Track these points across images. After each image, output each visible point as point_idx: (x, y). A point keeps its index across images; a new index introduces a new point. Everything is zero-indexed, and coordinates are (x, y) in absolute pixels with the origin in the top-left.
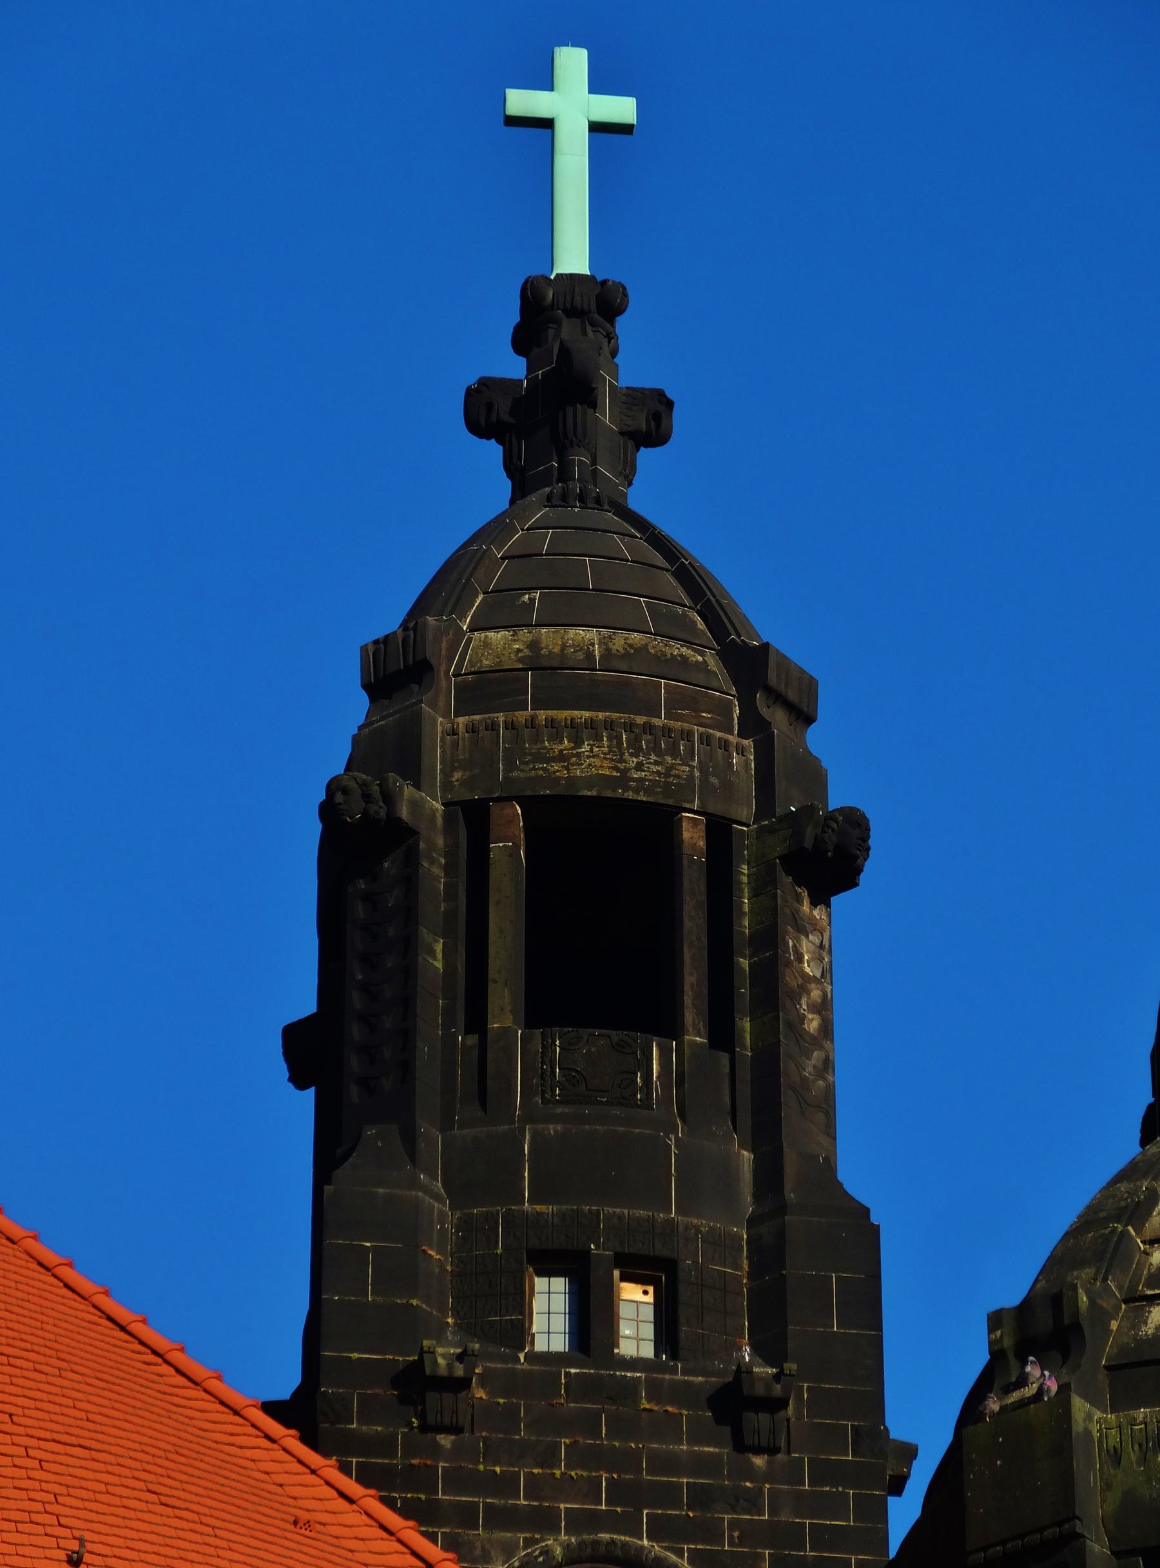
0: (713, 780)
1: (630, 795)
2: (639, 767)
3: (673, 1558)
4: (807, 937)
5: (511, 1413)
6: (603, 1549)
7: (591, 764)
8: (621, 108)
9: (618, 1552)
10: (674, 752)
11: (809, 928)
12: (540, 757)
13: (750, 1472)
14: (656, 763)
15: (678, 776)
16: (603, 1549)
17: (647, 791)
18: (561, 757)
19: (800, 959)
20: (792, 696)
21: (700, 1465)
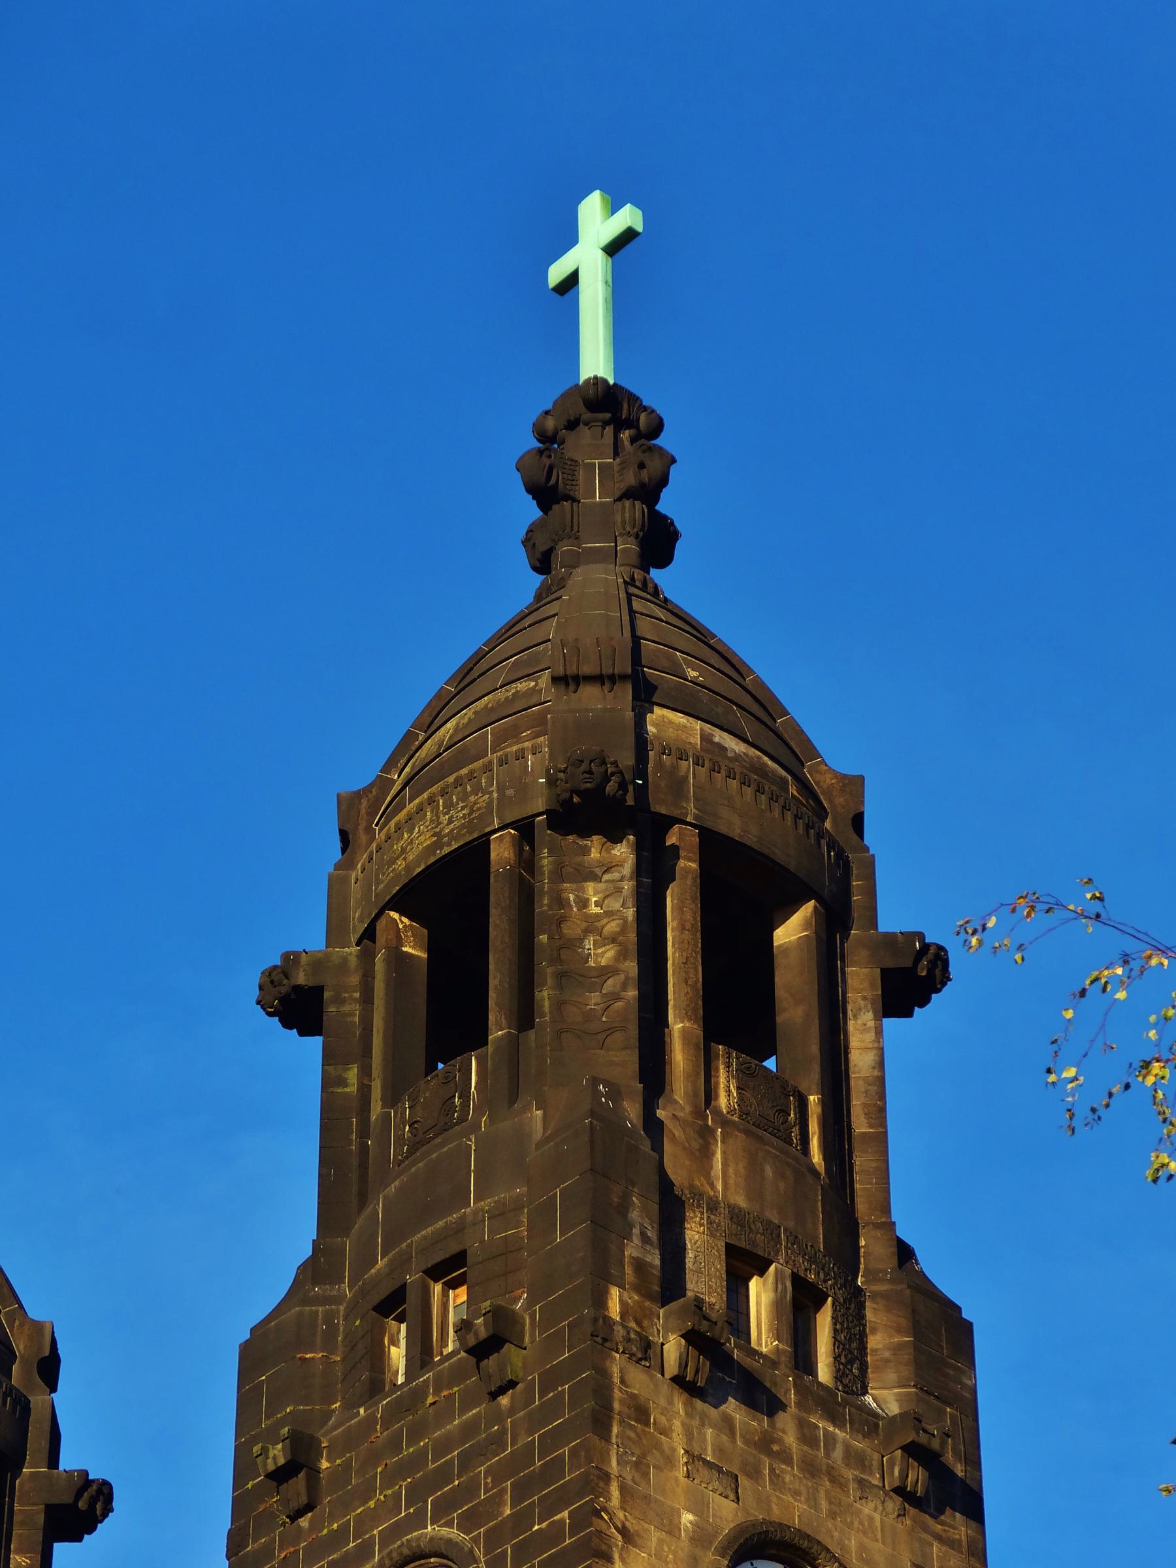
0: (510, 792)
1: (446, 850)
2: (450, 822)
3: (445, 1531)
4: (596, 878)
5: (347, 1465)
6: (395, 1555)
7: (418, 842)
8: (629, 217)
9: (406, 1551)
10: (477, 789)
11: (599, 871)
12: (393, 861)
13: (498, 1417)
14: (463, 808)
15: (479, 809)
16: (395, 1555)
17: (456, 839)
18: (403, 850)
19: (583, 903)
20: (587, 669)
21: (470, 1429)
